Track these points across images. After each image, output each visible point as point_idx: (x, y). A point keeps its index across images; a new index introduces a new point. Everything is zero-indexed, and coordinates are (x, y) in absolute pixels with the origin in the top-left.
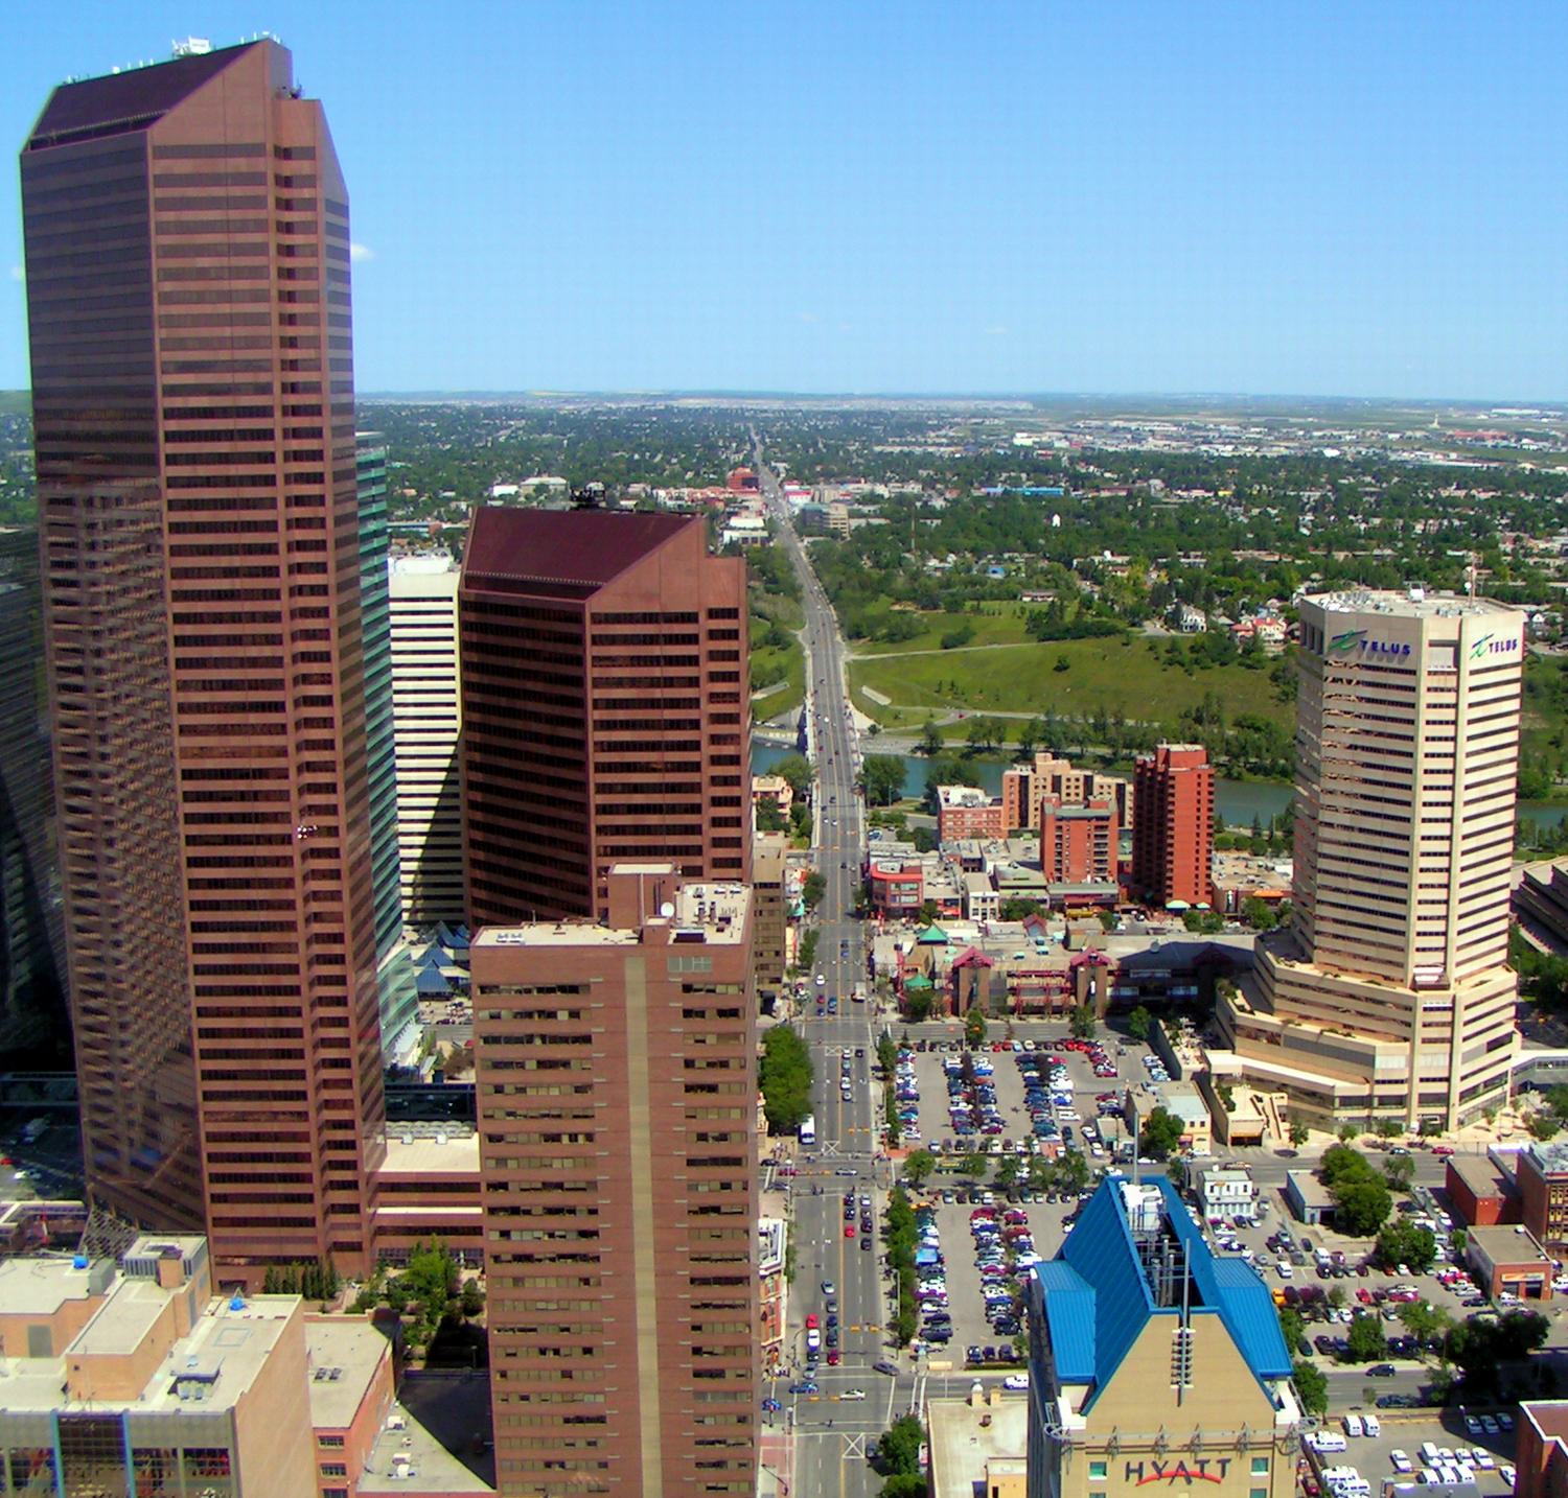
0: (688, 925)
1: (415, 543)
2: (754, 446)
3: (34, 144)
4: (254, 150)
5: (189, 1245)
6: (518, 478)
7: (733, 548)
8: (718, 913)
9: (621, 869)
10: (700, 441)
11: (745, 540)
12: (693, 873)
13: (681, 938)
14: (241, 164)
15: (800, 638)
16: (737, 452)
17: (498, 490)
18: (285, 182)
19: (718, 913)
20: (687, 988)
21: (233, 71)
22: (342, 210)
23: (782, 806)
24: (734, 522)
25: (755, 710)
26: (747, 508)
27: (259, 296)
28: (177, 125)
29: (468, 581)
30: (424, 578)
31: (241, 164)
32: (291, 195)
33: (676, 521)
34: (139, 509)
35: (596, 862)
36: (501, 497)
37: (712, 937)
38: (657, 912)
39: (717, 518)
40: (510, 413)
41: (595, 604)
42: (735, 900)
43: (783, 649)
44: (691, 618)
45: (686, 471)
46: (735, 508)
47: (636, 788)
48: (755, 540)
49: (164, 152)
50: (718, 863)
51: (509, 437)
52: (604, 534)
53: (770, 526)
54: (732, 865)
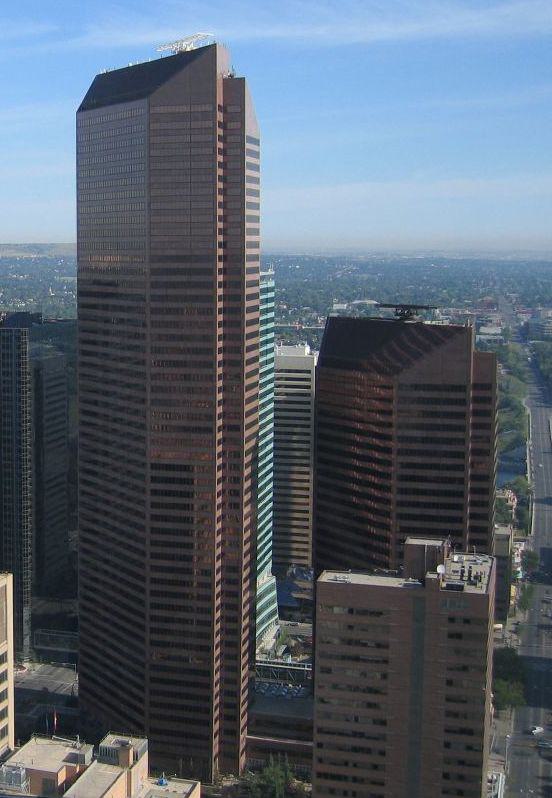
0: (455, 580)
2: (495, 282)
8: (473, 573)
11: (489, 341)
12: (458, 547)
13: (449, 587)
15: (523, 404)
16: (484, 286)
17: (336, 307)
19: (473, 573)
20: (452, 620)
23: (511, 508)
24: (483, 329)
26: (491, 321)
36: (338, 311)
38: (434, 570)
42: (484, 566)
43: (513, 410)
44: (462, 388)
45: (452, 297)
47: (424, 492)
48: (495, 341)
50: (472, 542)
51: (343, 274)
53: (505, 332)
54: (481, 543)
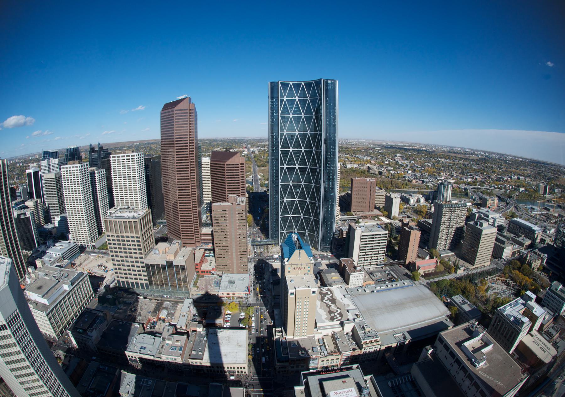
1: (205, 156)
3: (162, 110)
4: (187, 110)
5: (179, 241)
6: (217, 148)
7: (244, 156)
9: (230, 195)
10: (239, 142)
14: (185, 111)
18: (190, 113)
21: (184, 101)
22: (196, 116)
25: (246, 176)
27: (187, 127)
28: (178, 107)
29: (211, 160)
30: (206, 160)
31: (185, 111)
32: (192, 114)
33: (235, 153)
34: (173, 152)
35: (227, 195)
37: (241, 204)
39: (241, 152)
40: (216, 140)
41: (227, 163)
46: (244, 151)
49: (176, 110)
52: (228, 154)
